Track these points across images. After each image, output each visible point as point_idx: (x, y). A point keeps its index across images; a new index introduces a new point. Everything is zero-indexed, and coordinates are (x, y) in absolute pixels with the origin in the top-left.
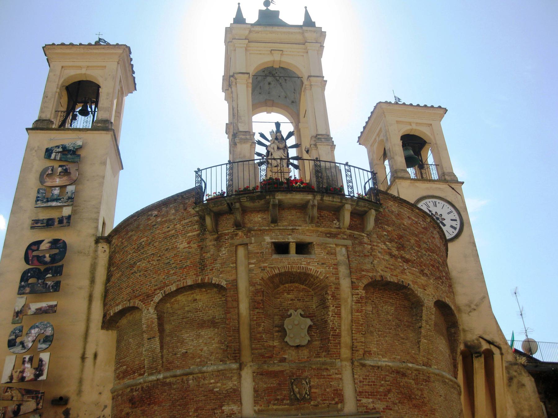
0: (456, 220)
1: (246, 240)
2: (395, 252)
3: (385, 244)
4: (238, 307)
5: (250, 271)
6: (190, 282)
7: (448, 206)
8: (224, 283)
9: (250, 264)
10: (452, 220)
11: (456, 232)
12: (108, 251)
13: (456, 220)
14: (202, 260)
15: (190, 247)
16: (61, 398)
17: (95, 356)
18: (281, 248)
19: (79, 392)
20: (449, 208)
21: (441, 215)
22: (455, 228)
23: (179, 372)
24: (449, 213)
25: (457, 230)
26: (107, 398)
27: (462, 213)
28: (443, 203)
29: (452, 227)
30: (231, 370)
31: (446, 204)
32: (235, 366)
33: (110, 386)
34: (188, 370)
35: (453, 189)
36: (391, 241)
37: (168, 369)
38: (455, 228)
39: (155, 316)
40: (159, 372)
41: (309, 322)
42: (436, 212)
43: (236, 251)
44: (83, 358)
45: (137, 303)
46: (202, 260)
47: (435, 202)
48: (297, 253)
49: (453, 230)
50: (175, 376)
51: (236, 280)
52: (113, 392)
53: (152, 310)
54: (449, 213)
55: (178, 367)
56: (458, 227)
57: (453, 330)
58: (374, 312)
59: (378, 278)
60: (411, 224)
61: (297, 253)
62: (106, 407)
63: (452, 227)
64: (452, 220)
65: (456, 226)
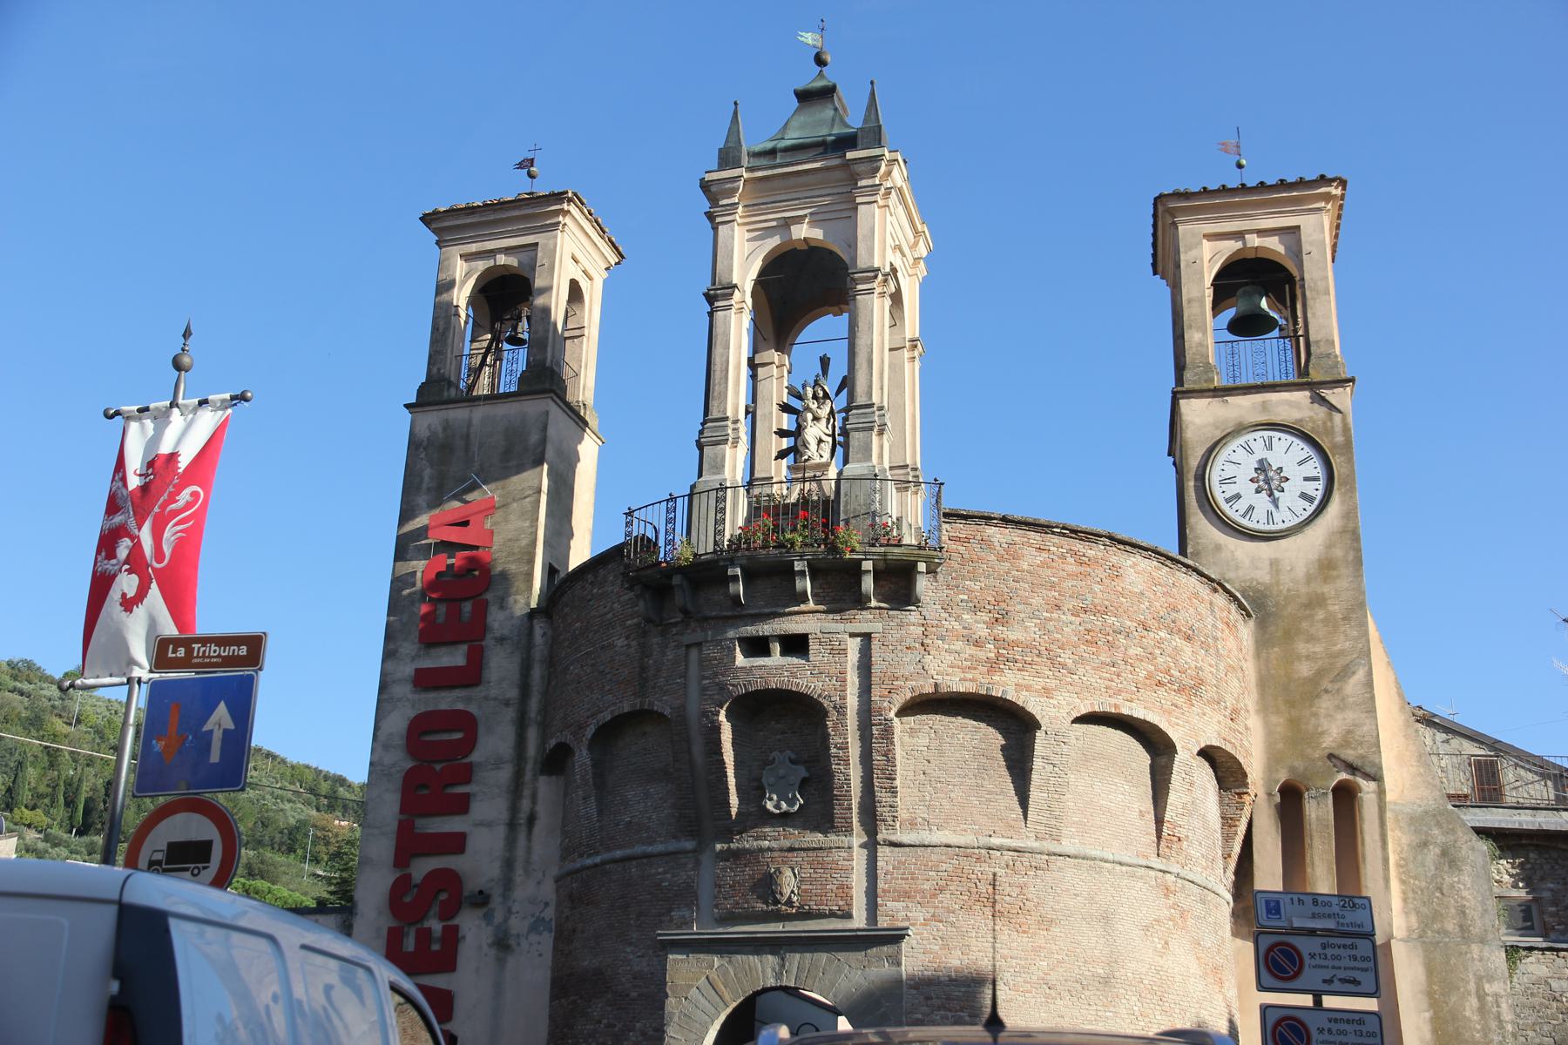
1: (698, 636)
2: (982, 631)
3: (958, 618)
4: (689, 751)
5: (704, 689)
6: (626, 708)
7: (1302, 444)
8: (667, 712)
9: (705, 678)
10: (1306, 479)
11: (1311, 508)
12: (549, 633)
14: (643, 669)
15: (629, 646)
16: (481, 892)
17: (532, 819)
18: (758, 647)
19: (507, 883)
20: (1300, 449)
22: (1310, 499)
23: (618, 854)
24: (1300, 463)
25: (1316, 502)
26: (548, 890)
27: (1336, 461)
28: (1290, 438)
29: (1304, 496)
30: (685, 852)
31: (1297, 441)
32: (689, 845)
33: (555, 871)
34: (628, 852)
36: (975, 610)
37: (609, 849)
39: (588, 761)
40: (597, 853)
41: (802, 772)
43: (687, 655)
44: (512, 825)
45: (567, 737)
46: (643, 669)
47: (1271, 438)
48: (783, 653)
50: (615, 861)
51: (683, 707)
52: (557, 880)
53: (585, 752)
54: (1300, 463)
55: (620, 847)
56: (1319, 495)
57: (1163, 760)
58: (933, 746)
59: (929, 689)
60: (1043, 565)
61: (783, 653)
62: (547, 904)
63: (1304, 496)
64: (1306, 479)
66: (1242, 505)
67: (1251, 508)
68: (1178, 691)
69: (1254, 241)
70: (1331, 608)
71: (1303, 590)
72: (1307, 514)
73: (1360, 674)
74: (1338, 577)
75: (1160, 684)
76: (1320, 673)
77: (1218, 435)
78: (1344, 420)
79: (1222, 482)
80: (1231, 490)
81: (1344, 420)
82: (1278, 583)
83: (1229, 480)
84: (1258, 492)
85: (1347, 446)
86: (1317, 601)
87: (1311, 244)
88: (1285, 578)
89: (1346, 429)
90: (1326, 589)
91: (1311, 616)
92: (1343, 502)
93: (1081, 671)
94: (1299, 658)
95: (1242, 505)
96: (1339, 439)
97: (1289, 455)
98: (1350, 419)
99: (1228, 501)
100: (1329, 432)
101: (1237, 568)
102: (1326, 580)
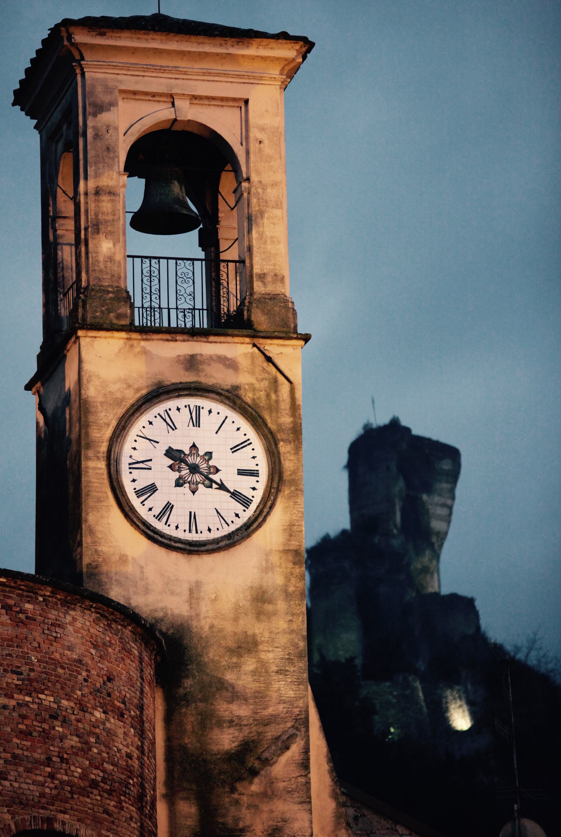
0: (253, 473)
13: (253, 473)
21: (209, 454)
22: (245, 502)
25: (253, 507)
35: (269, 359)
38: (245, 502)
42: (194, 446)
47: (198, 409)
49: (239, 508)
56: (257, 497)
65: (248, 493)
66: (157, 502)
67: (169, 507)
68: (110, 792)
69: (190, 112)
70: (263, 656)
71: (229, 627)
72: (239, 523)
73: (295, 749)
74: (275, 613)
75: (94, 784)
76: (247, 748)
77: (132, 397)
78: (292, 391)
79: (133, 466)
80: (144, 479)
81: (292, 391)
82: (198, 615)
83: (143, 465)
84: (179, 483)
85: (296, 431)
86: (246, 646)
87: (262, 129)
88: (205, 608)
89: (294, 407)
90: (259, 629)
91: (237, 666)
92: (286, 508)
93: (13, 775)
94: (220, 723)
95: (157, 502)
96: (286, 420)
97: (222, 434)
98: (299, 394)
99: (139, 493)
100: (274, 408)
101: (147, 590)
102: (260, 615)
